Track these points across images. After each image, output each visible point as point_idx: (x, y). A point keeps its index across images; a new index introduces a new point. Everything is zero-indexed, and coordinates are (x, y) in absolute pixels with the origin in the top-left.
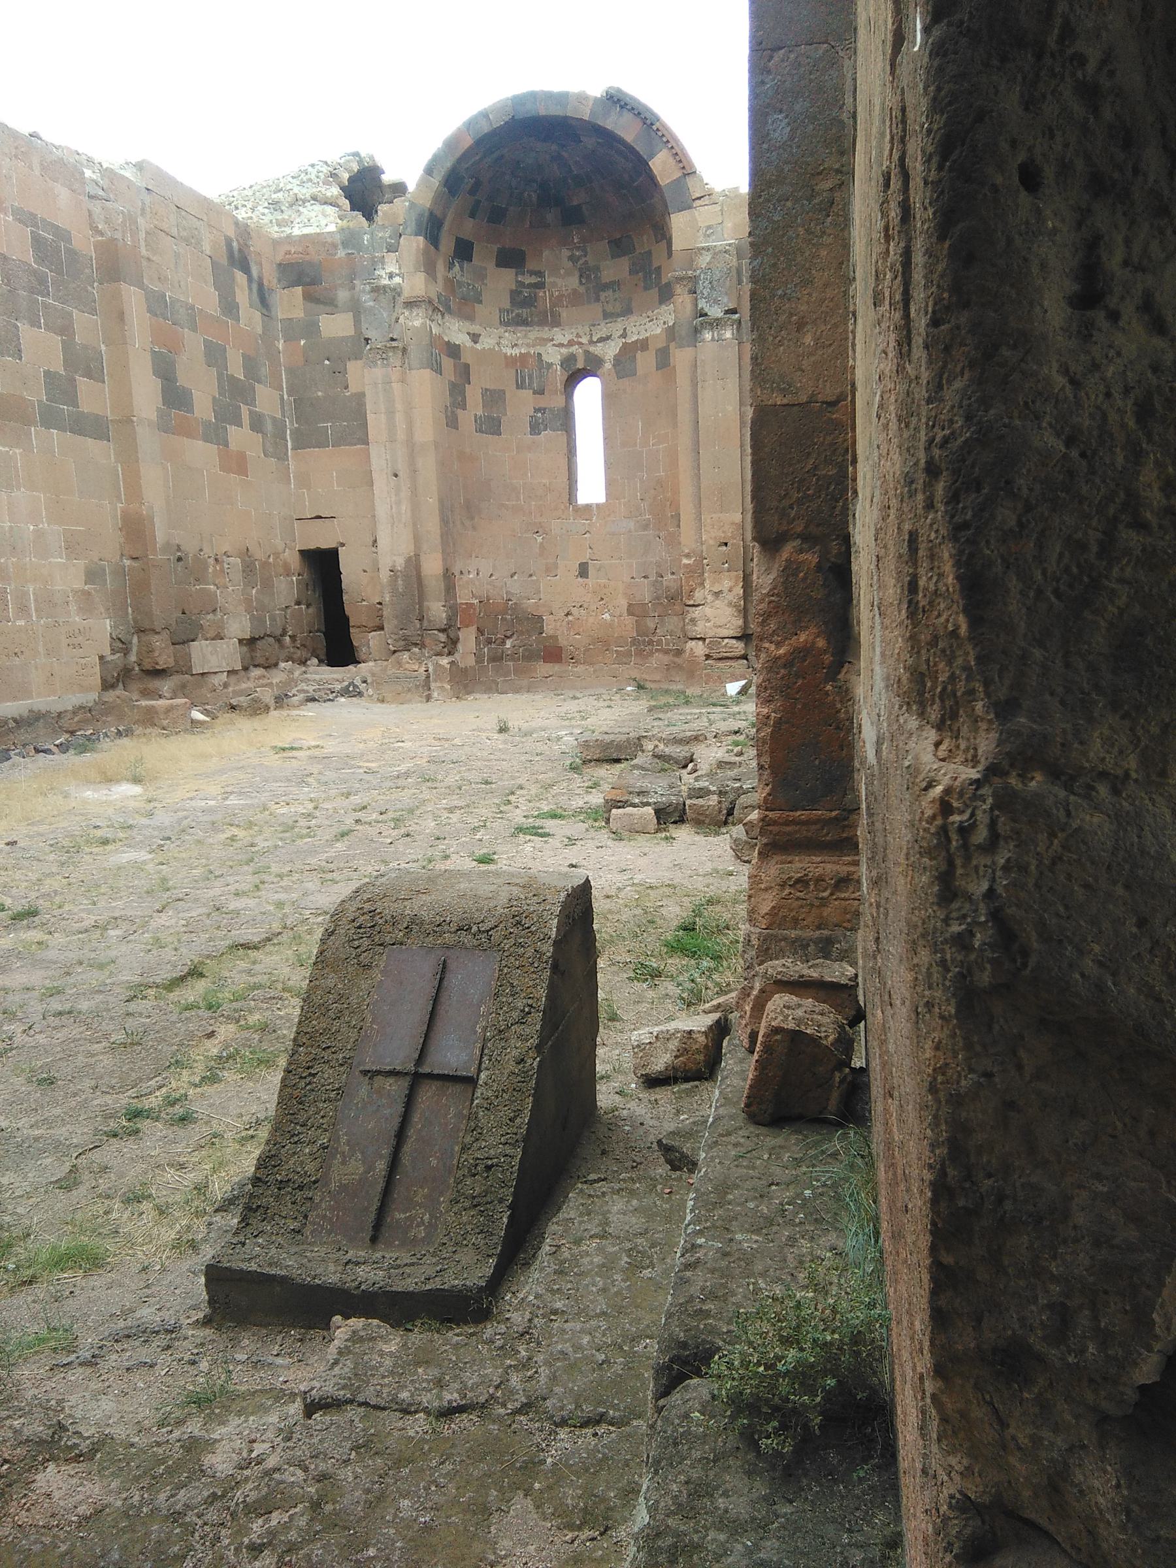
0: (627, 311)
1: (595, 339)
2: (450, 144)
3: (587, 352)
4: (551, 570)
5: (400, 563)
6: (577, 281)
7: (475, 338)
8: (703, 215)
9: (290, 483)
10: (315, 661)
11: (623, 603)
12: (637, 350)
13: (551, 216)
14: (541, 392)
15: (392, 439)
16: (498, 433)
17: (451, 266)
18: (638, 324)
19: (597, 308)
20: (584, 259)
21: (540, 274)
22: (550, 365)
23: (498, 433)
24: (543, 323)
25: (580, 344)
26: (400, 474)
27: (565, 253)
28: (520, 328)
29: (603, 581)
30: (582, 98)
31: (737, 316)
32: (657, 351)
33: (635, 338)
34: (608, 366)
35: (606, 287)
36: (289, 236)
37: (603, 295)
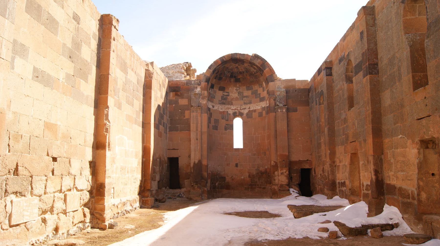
0: (250, 103)
1: (241, 109)
2: (215, 62)
3: (239, 112)
4: (228, 165)
5: (197, 162)
6: (237, 95)
7: (213, 107)
8: (277, 83)
9: (167, 140)
10: (168, 187)
11: (247, 174)
12: (253, 112)
13: (232, 80)
14: (227, 120)
15: (197, 130)
16: (217, 130)
17: (209, 90)
19: (242, 102)
20: (239, 90)
22: (230, 114)
23: (217, 130)
24: (229, 104)
25: (238, 110)
26: (198, 139)
27: (235, 88)
28: (223, 105)
30: (247, 55)
31: (287, 106)
34: (245, 115)
35: (245, 97)
36: (173, 81)
37: (244, 99)
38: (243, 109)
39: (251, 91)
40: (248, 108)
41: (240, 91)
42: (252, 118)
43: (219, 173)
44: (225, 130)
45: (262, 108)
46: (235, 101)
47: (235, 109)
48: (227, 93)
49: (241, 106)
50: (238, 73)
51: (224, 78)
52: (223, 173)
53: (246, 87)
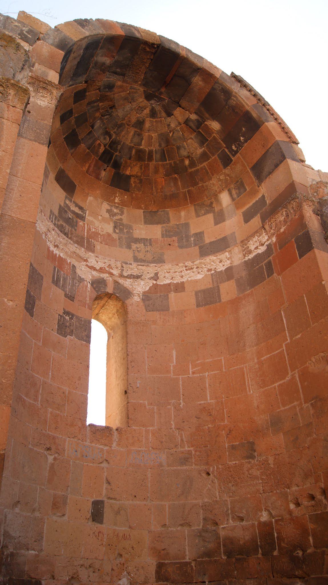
0: (159, 260)
1: (125, 274)
3: (116, 282)
12: (170, 292)
18: (171, 271)
19: (128, 254)
20: (119, 217)
21: (81, 208)
22: (81, 280)
25: (111, 274)
27: (105, 206)
29: (122, 529)
32: (197, 293)
33: (168, 281)
37: (134, 246)
38: (130, 277)
39: (162, 227)
40: (152, 275)
41: (121, 220)
42: (168, 309)
43: (12, 555)
44: (61, 334)
45: (212, 274)
46: (101, 243)
47: (101, 268)
48: (77, 208)
49: (124, 265)
50: (134, 152)
51: (83, 145)
52: (33, 552)
53: (144, 212)
